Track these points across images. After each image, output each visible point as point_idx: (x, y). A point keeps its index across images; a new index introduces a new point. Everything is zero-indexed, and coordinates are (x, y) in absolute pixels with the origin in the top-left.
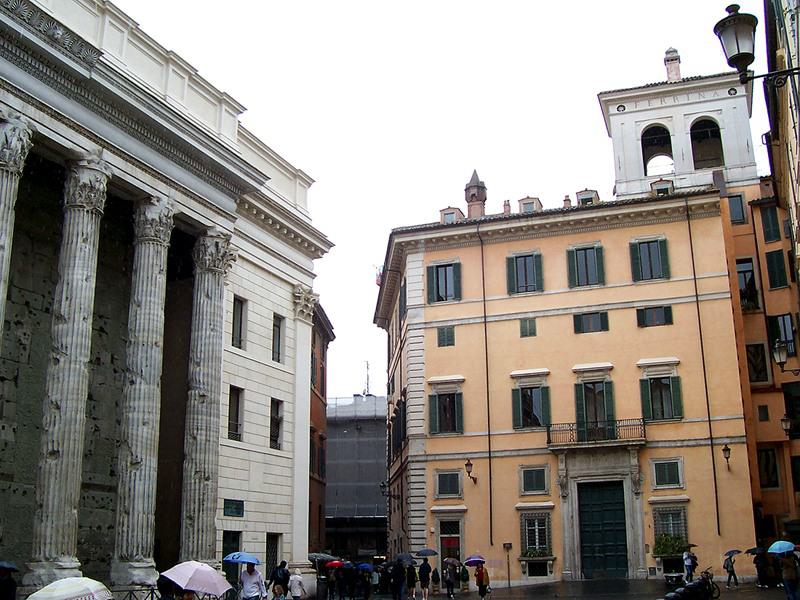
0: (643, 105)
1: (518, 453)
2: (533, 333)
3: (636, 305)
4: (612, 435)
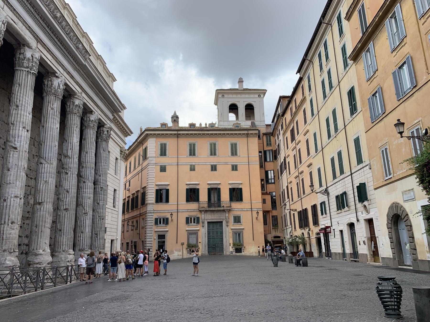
0: (230, 96)
1: (188, 211)
2: (194, 170)
4: (219, 206)
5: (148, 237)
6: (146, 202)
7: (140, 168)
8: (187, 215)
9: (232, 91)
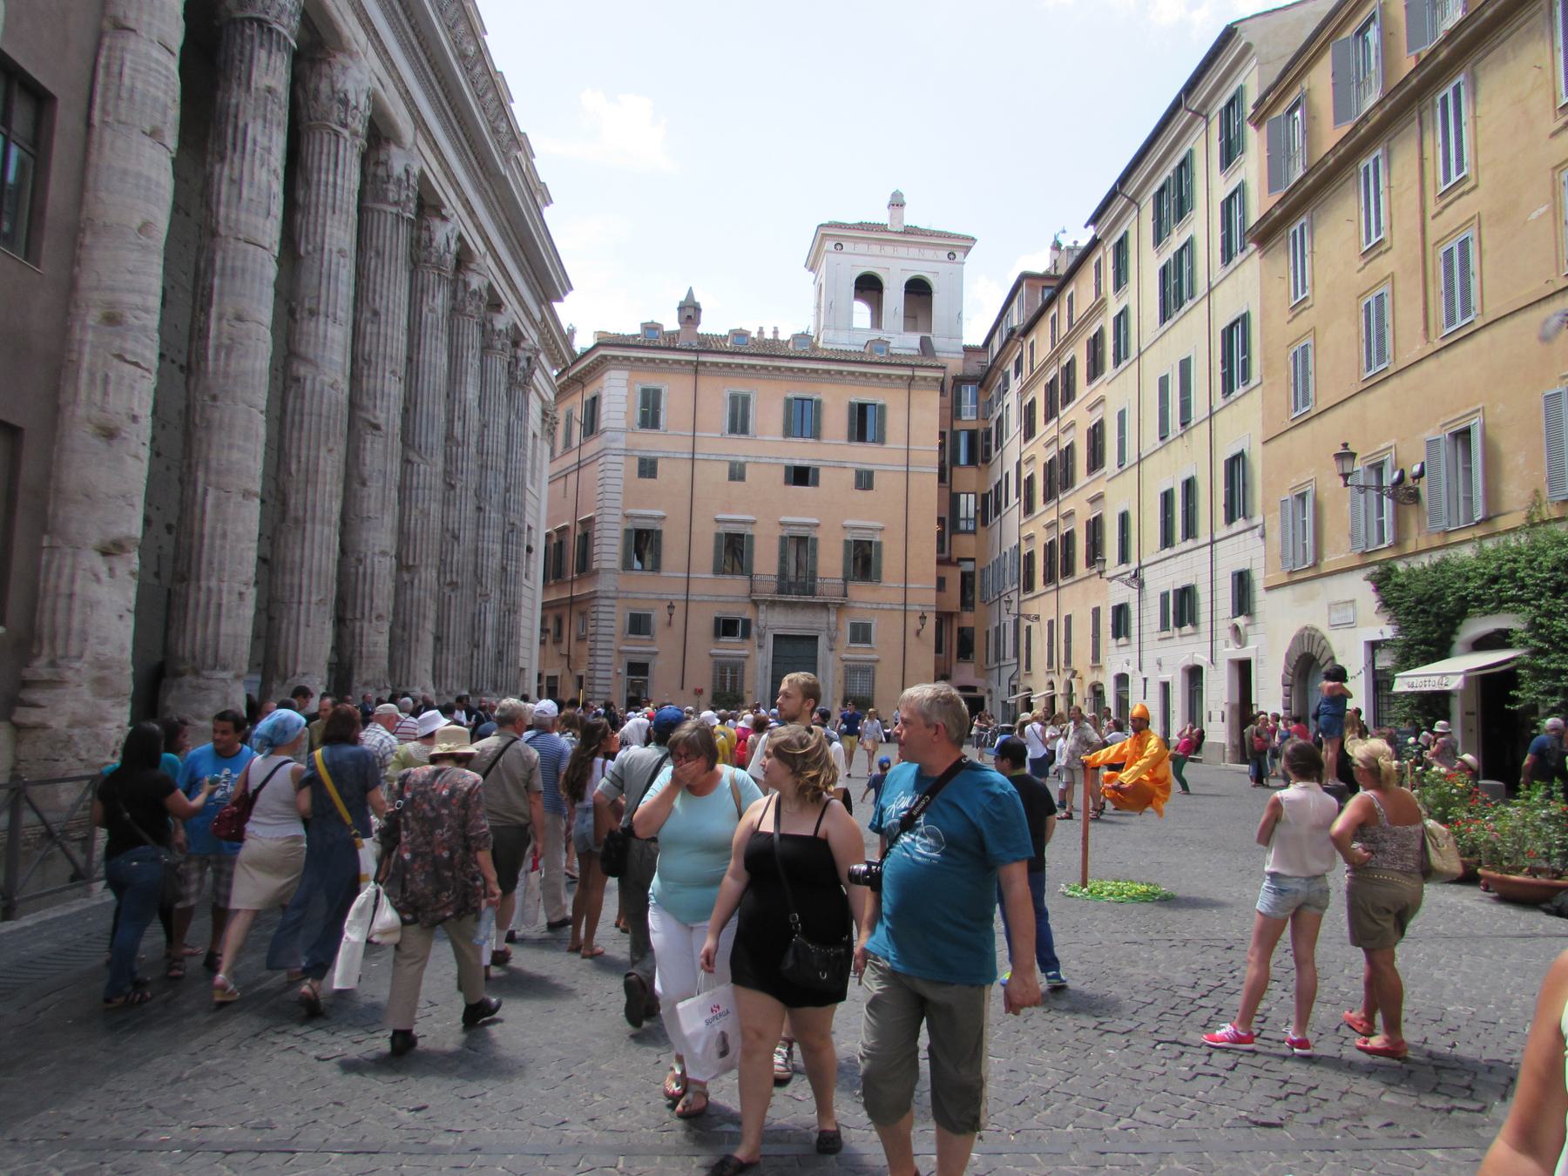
0: (862, 248)
2: (742, 478)
4: (812, 592)
6: (595, 566)
7: (572, 459)
9: (868, 231)
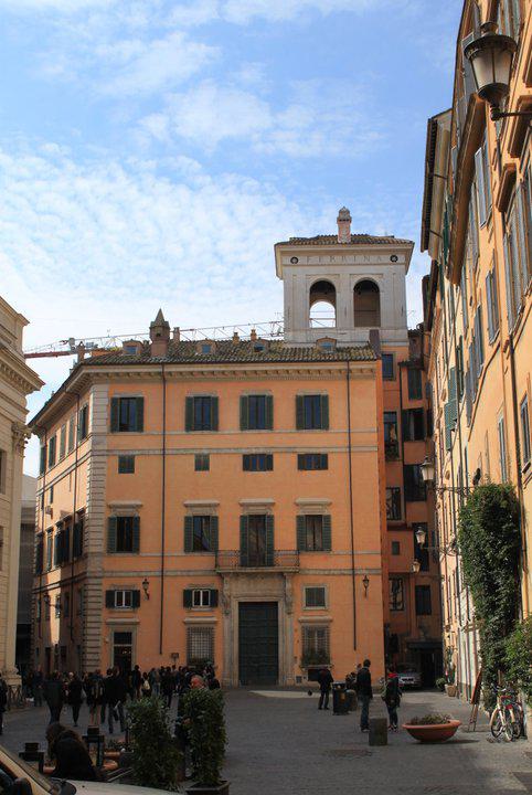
0: (314, 259)
3: (297, 450)
5: (89, 638)
6: (84, 552)
7: (71, 460)
8: (186, 584)
